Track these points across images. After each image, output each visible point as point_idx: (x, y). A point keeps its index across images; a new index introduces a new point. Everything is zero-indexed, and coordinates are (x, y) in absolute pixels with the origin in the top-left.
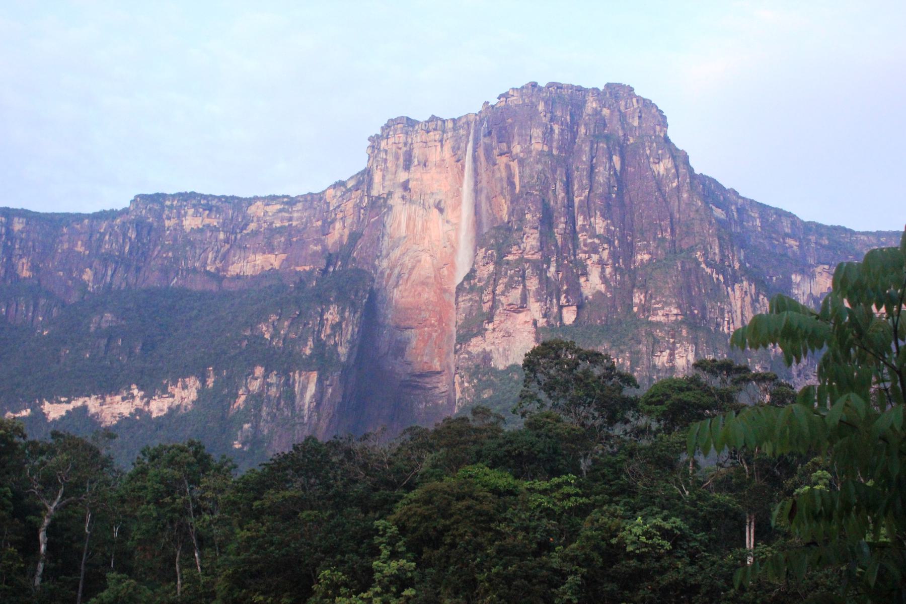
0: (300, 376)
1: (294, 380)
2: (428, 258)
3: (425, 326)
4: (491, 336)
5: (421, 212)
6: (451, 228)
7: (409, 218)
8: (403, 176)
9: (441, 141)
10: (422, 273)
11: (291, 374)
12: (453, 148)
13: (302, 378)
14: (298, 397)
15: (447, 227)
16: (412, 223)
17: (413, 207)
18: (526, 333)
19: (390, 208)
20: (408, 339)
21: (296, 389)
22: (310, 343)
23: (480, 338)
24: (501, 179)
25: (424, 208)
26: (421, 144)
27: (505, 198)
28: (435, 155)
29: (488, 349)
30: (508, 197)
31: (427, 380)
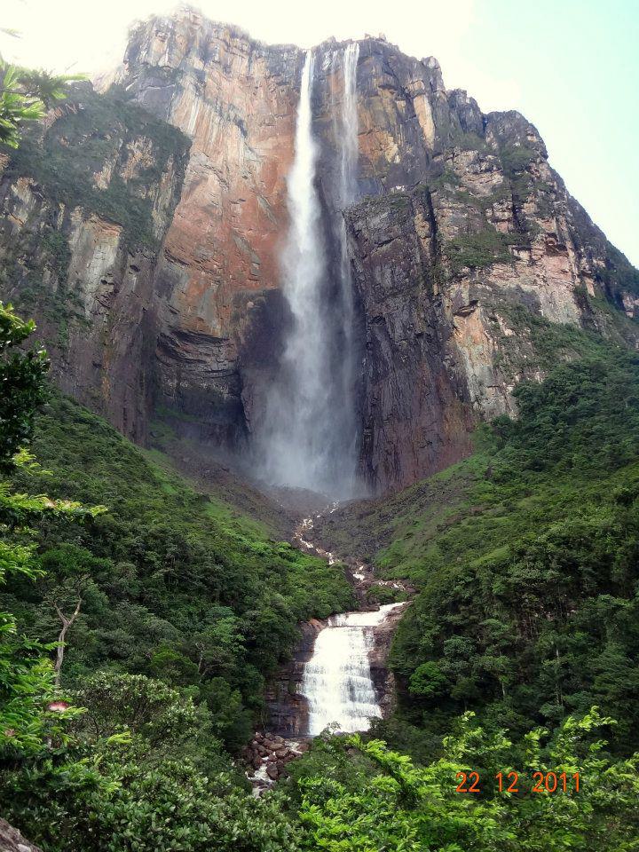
0: (86, 218)
1: (67, 221)
2: (216, 183)
3: (203, 269)
4: (528, 270)
5: (217, 119)
7: (202, 117)
8: (198, 64)
11: (62, 206)
12: (272, 69)
13: (89, 226)
14: (75, 258)
15: (249, 155)
16: (204, 125)
19: (180, 89)
20: (178, 276)
21: (72, 242)
22: (107, 172)
23: (508, 268)
24: (386, 115)
25: (221, 115)
26: (223, 43)
27: (393, 135)
28: (240, 65)
29: (527, 288)
30: (401, 136)
31: (190, 347)
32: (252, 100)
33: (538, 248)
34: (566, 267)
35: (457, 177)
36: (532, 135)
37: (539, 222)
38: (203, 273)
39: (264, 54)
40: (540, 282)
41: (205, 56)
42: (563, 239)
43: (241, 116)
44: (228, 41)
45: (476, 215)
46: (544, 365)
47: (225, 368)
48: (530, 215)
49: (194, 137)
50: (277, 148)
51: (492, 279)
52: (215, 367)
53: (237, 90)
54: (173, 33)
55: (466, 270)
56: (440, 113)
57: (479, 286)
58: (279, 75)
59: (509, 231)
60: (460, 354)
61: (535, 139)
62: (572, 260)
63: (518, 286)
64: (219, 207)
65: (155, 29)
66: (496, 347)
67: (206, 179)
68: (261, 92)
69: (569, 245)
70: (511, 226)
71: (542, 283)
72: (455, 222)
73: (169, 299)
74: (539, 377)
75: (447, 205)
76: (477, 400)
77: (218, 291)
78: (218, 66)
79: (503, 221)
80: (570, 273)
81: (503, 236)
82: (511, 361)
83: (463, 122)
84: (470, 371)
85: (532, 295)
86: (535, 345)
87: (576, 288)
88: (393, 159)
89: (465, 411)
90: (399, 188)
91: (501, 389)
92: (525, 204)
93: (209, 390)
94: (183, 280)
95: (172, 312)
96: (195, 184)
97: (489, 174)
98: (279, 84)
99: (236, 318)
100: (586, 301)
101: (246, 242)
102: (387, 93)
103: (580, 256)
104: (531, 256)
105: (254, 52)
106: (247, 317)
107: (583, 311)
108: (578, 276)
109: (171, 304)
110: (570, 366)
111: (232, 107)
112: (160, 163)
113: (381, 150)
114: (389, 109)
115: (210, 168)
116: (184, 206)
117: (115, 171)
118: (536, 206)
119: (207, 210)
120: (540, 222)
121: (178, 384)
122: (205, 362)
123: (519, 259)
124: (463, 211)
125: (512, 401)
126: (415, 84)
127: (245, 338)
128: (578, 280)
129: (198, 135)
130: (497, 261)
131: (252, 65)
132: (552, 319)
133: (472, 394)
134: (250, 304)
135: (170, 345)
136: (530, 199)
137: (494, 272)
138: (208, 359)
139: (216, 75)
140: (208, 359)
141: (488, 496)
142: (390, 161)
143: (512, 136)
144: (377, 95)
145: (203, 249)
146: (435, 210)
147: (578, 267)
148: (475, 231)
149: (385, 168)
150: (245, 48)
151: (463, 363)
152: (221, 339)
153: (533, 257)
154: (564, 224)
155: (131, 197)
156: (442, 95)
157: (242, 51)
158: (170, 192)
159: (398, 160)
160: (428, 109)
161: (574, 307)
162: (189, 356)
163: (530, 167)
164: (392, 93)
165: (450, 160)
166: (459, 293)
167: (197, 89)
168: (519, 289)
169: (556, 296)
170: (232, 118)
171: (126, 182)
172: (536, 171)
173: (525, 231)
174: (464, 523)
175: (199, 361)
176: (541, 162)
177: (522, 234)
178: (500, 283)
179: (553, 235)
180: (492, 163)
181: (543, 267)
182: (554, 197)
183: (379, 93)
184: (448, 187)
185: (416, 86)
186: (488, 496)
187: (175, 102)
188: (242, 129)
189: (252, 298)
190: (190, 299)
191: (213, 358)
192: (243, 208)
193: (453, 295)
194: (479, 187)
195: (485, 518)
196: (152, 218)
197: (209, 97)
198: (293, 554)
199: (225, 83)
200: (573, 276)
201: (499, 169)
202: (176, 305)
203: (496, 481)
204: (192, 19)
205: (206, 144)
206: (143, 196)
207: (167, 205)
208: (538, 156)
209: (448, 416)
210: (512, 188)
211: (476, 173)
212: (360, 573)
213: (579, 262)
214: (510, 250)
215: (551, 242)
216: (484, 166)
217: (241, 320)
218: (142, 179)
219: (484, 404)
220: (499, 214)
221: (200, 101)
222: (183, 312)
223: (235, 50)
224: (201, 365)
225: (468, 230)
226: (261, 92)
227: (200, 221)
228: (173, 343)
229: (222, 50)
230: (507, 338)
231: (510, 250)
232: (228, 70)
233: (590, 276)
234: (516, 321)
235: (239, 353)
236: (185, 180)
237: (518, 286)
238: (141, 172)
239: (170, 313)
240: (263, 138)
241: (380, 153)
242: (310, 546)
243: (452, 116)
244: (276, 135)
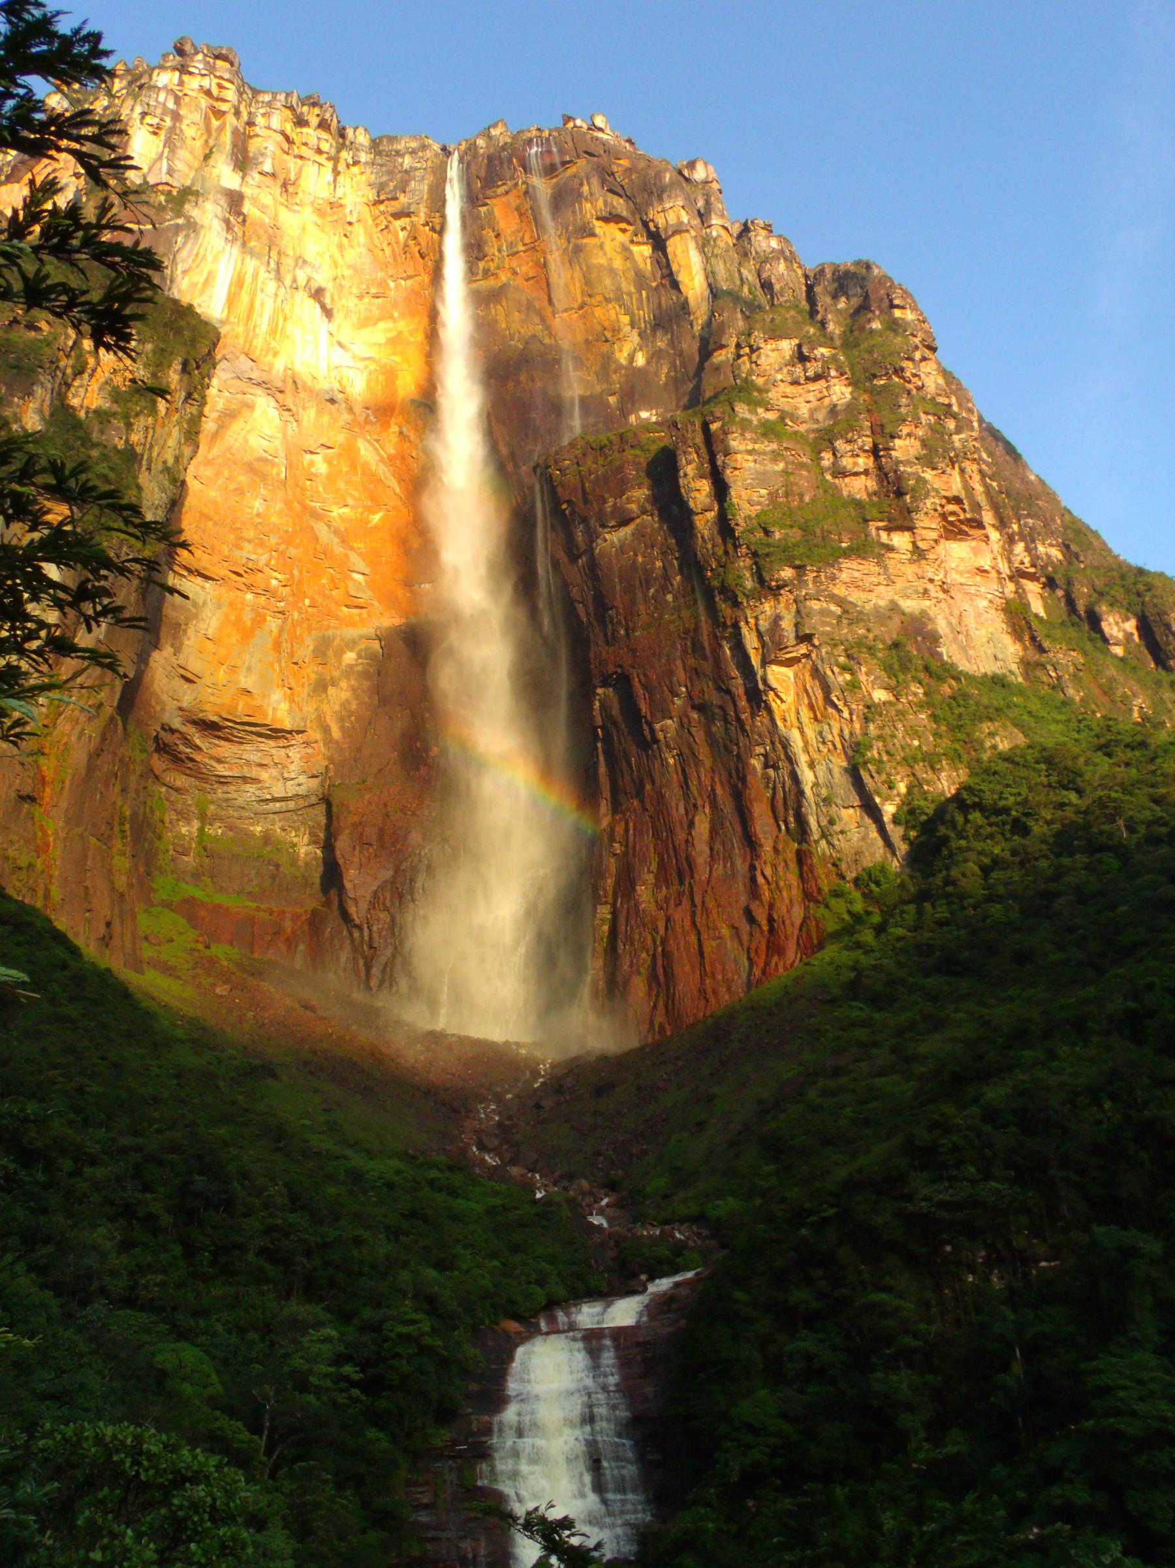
2: (273, 413)
3: (249, 587)
4: (910, 570)
5: (272, 286)
6: (352, 363)
7: (239, 283)
8: (229, 178)
9: (335, 160)
10: (254, 441)
12: (381, 188)
15: (339, 356)
16: (245, 297)
17: (251, 264)
18: (985, 603)
22: (42, 395)
23: (871, 566)
24: (612, 271)
25: (279, 278)
26: (280, 138)
29: (910, 605)
31: (226, 749)
32: (341, 247)
33: (928, 525)
34: (986, 563)
35: (760, 390)
36: (903, 308)
37: (928, 475)
38: (249, 596)
39: (363, 157)
40: (934, 591)
41: (243, 161)
42: (977, 507)
43: (322, 279)
44: (288, 132)
45: (802, 466)
46: (955, 758)
47: (302, 791)
48: (908, 463)
49: (223, 322)
50: (394, 342)
51: (840, 590)
52: (279, 790)
53: (311, 228)
54: (177, 117)
55: (787, 573)
56: (721, 269)
57: (815, 605)
58: (396, 199)
59: (869, 495)
60: (786, 744)
61: (909, 316)
62: (996, 547)
63: (892, 602)
64: (282, 454)
65: (138, 109)
66: (857, 726)
67: (251, 407)
68: (359, 234)
69: (988, 517)
70: (871, 484)
71: (941, 595)
72: (762, 479)
73: (177, 650)
74: (946, 783)
75: (742, 447)
76: (824, 835)
77: (280, 634)
78: (268, 180)
79: (856, 474)
80: (994, 574)
81: (858, 504)
82: (888, 753)
83: (767, 286)
84: (807, 777)
85: (924, 613)
86: (934, 718)
87: (1008, 602)
88: (631, 358)
89: (802, 858)
90: (644, 415)
91: (872, 811)
92: (897, 441)
93: (267, 838)
94: (207, 613)
95: (183, 677)
96: (229, 416)
97: (823, 383)
98: (397, 216)
99: (321, 686)
100: (1030, 628)
101: (336, 532)
102: (612, 229)
103: (1011, 540)
104: (914, 543)
105: (344, 154)
106: (343, 684)
107: (1025, 648)
108: (1011, 578)
109: (182, 662)
110: (1007, 758)
111: (301, 261)
112: (154, 375)
113: (607, 341)
114: (618, 263)
115: (259, 384)
116: (208, 462)
117: (59, 394)
118: (918, 444)
119: (257, 469)
120: (928, 475)
121: (201, 830)
122: (256, 780)
123: (890, 549)
124: (776, 456)
125: (896, 833)
126: (672, 212)
127: (342, 728)
128: (1010, 587)
129: (232, 319)
130: (847, 554)
131: (340, 178)
132: (964, 666)
133: (812, 821)
134: (350, 657)
135: (182, 748)
136: (905, 430)
137: (844, 576)
138: (264, 775)
139: (266, 199)
140: (264, 775)
141: (859, 1033)
142: (624, 362)
143: (864, 308)
144: (593, 235)
145: (248, 547)
146: (720, 459)
147: (1010, 561)
148: (801, 500)
149: (615, 377)
150: (325, 147)
151: (791, 760)
152: (290, 732)
153: (921, 544)
154: (976, 477)
155: (97, 445)
156: (723, 233)
157: (319, 151)
158: (175, 432)
159: (640, 360)
160: (695, 259)
161: (1007, 640)
162: (222, 770)
163: (902, 370)
164: (624, 231)
165: (746, 358)
166: (777, 619)
167: (229, 227)
168: (894, 607)
169: (970, 621)
170: (302, 281)
171: (82, 414)
172: (915, 375)
173: (900, 494)
174: (812, 1094)
175: (245, 779)
176: (924, 359)
177: (896, 498)
178: (855, 597)
179: (957, 500)
180: (826, 363)
181: (939, 563)
182: (951, 424)
183: (597, 231)
184: (742, 410)
185: (672, 218)
186: (859, 1033)
187: (184, 254)
188: (323, 307)
189: (351, 644)
190: (222, 652)
191: (274, 772)
192: (329, 461)
193: (764, 625)
194: (804, 411)
195: (855, 1080)
196: (139, 488)
197: (253, 243)
198: (458, 1180)
199: (286, 218)
200: (1000, 580)
201: (842, 375)
202: (195, 665)
203: (876, 1001)
204: (215, 91)
205: (250, 334)
206: (121, 445)
207: (171, 462)
208: (917, 348)
209: (768, 871)
210: (869, 411)
211: (795, 383)
212: (601, 1212)
213: (1011, 552)
214: (874, 532)
215: (953, 513)
216: (812, 369)
217: (331, 690)
218: (115, 408)
219: (840, 842)
220: (847, 462)
221: (236, 250)
222: (208, 680)
223: (305, 151)
224: (251, 788)
225: (787, 495)
226: (359, 232)
227: (239, 491)
228: (188, 743)
229: (279, 152)
230: (877, 706)
231: (874, 532)
232: (291, 189)
233: (1032, 577)
234: (888, 669)
235: (331, 760)
236: (206, 410)
237: (892, 602)
238: (116, 396)
239: (182, 681)
240: (365, 322)
241: (605, 348)
242: (490, 1160)
243: (745, 272)
244: (391, 317)
